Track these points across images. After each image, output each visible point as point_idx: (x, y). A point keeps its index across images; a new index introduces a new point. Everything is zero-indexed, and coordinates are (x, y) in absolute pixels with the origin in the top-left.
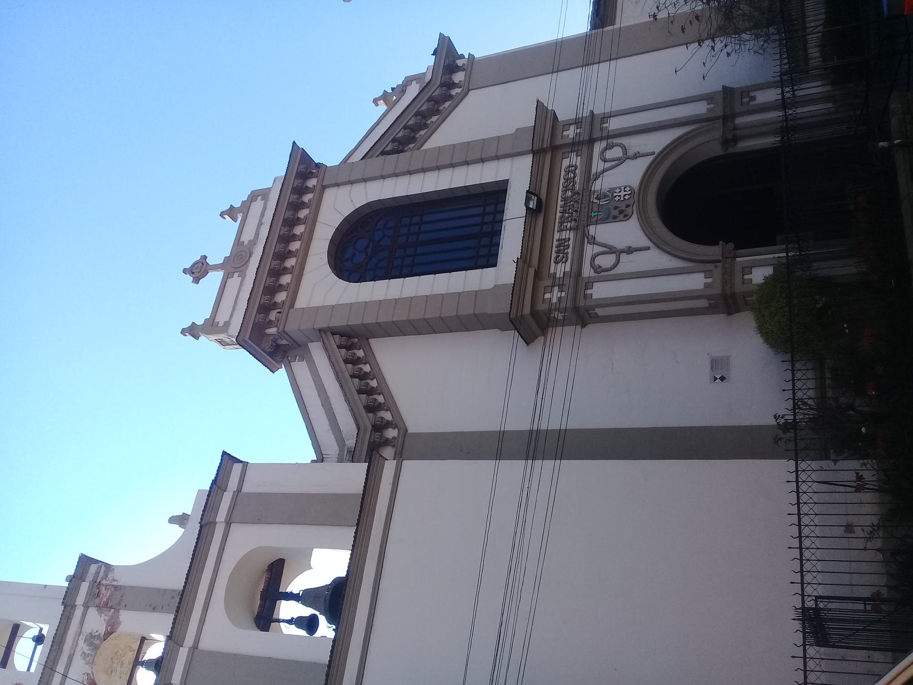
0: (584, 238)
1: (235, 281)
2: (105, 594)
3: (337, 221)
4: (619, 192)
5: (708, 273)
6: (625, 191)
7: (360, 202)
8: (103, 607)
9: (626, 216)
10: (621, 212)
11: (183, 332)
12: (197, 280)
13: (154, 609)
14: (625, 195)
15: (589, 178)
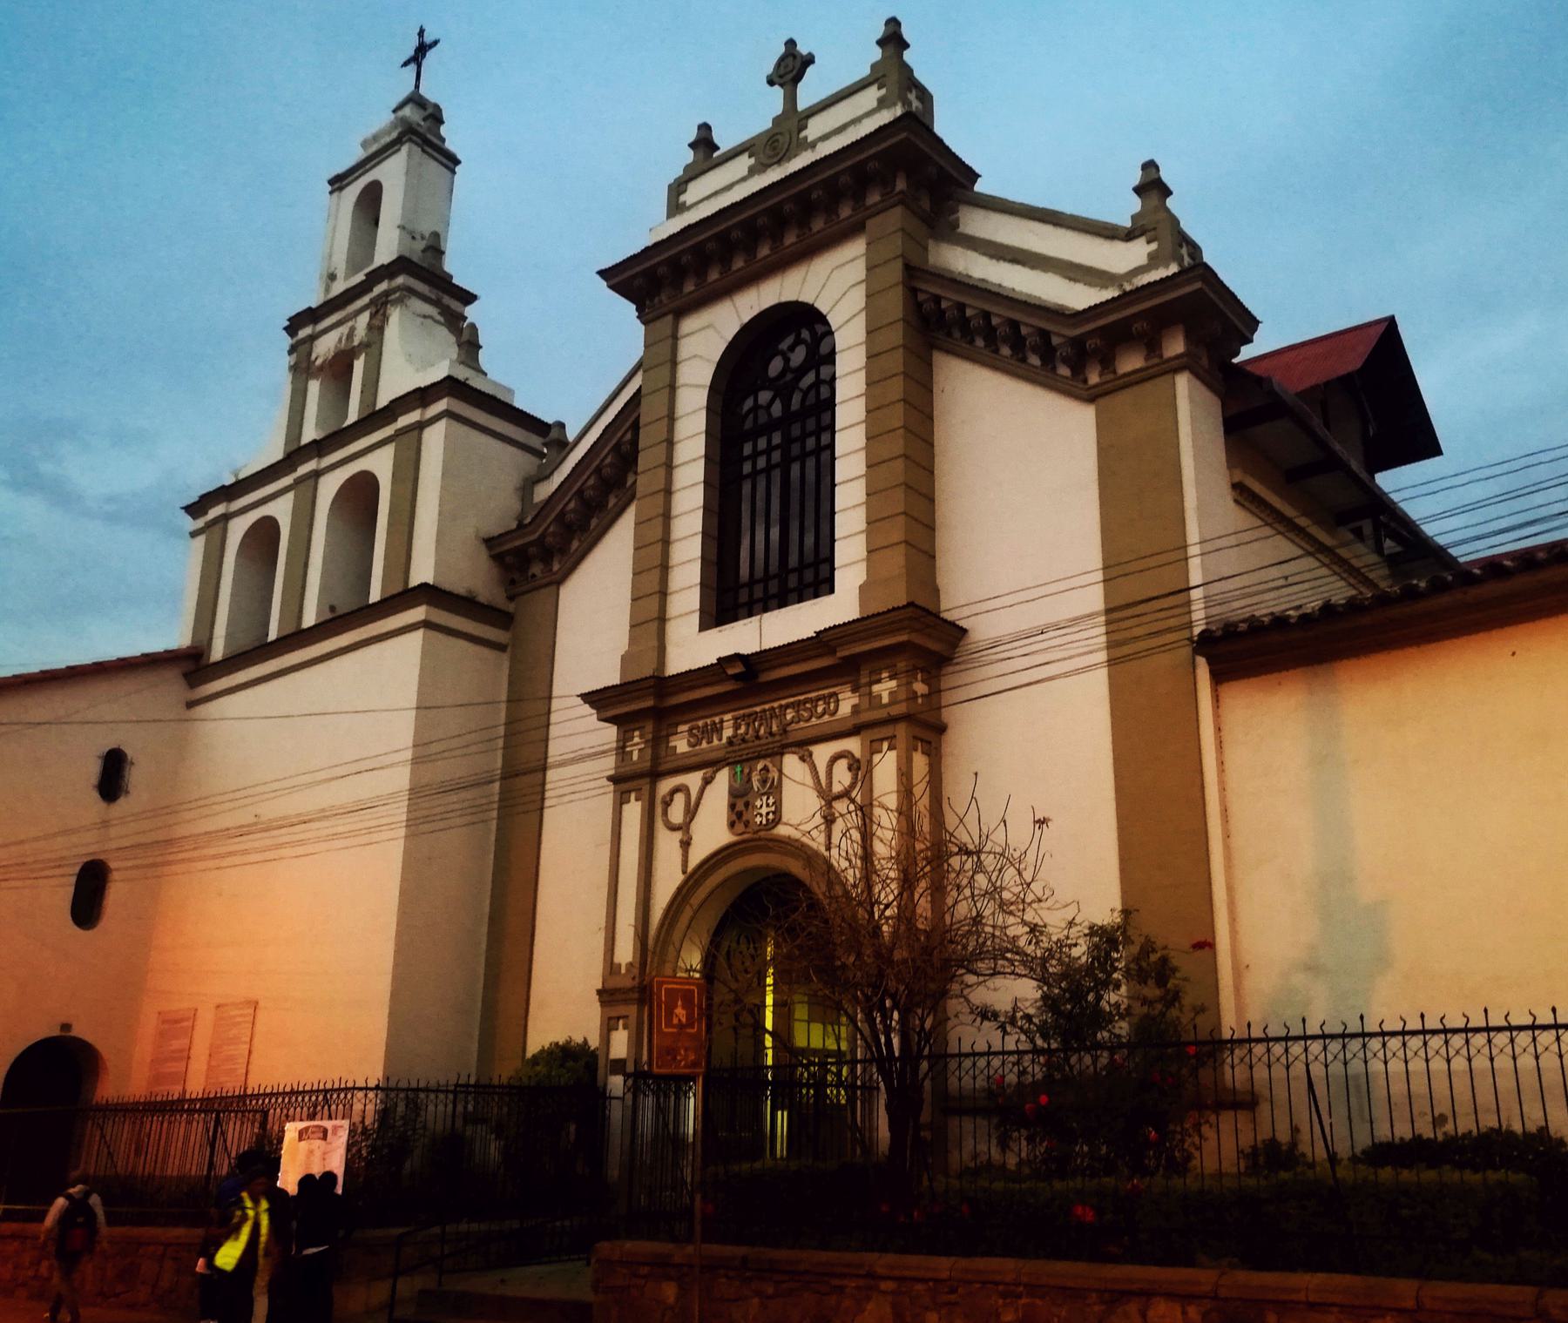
0: (710, 765)
1: (744, 163)
2: (376, 322)
3: (806, 298)
4: (768, 805)
5: (630, 965)
6: (768, 814)
7: (834, 321)
8: (370, 327)
9: (732, 825)
10: (740, 815)
11: (705, 128)
12: (771, 82)
13: (362, 392)
14: (761, 815)
15: (803, 746)
